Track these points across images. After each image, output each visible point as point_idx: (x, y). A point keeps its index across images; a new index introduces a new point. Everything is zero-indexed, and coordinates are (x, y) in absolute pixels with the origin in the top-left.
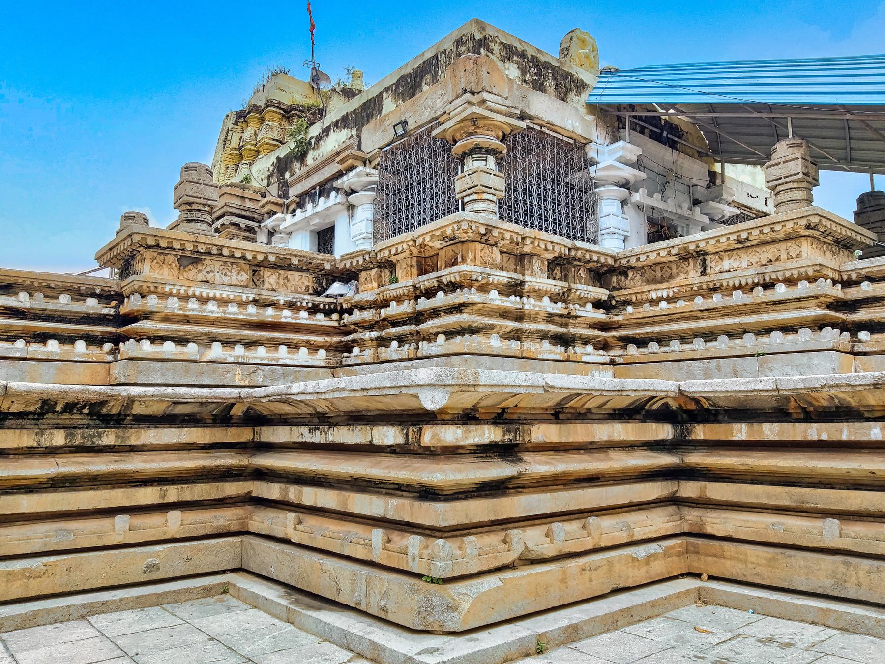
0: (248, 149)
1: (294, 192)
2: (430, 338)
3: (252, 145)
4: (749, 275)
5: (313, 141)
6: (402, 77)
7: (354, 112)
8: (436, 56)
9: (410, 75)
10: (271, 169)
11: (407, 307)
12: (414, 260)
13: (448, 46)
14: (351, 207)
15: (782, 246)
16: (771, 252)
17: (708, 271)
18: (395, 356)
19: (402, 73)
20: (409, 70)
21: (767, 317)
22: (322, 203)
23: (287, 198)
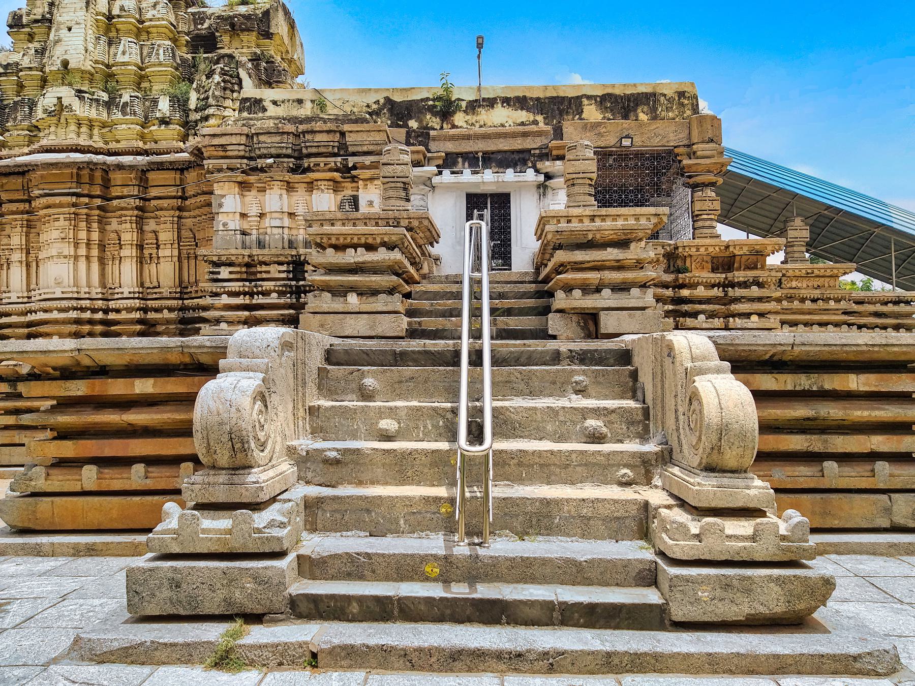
0: (130, 23)
1: (440, 148)
2: (748, 315)
3: (136, 19)
4: (816, 293)
5: (464, 104)
6: (610, 95)
7: (538, 99)
8: (654, 94)
9: (622, 98)
10: (375, 107)
11: (717, 292)
12: (708, 259)
13: (669, 92)
14: (543, 188)
15: (827, 279)
16: (820, 282)
17: (783, 286)
18: (705, 325)
19: (610, 91)
20: (617, 91)
21: (825, 318)
22: (509, 175)
23: (429, 151)
